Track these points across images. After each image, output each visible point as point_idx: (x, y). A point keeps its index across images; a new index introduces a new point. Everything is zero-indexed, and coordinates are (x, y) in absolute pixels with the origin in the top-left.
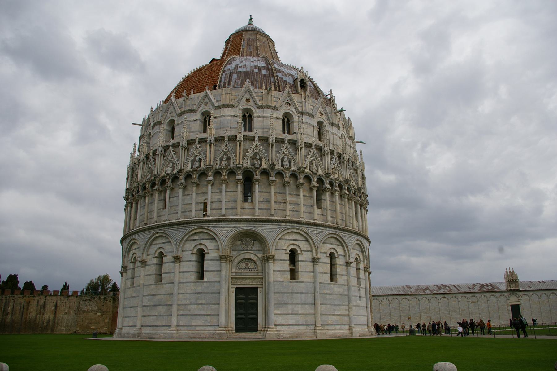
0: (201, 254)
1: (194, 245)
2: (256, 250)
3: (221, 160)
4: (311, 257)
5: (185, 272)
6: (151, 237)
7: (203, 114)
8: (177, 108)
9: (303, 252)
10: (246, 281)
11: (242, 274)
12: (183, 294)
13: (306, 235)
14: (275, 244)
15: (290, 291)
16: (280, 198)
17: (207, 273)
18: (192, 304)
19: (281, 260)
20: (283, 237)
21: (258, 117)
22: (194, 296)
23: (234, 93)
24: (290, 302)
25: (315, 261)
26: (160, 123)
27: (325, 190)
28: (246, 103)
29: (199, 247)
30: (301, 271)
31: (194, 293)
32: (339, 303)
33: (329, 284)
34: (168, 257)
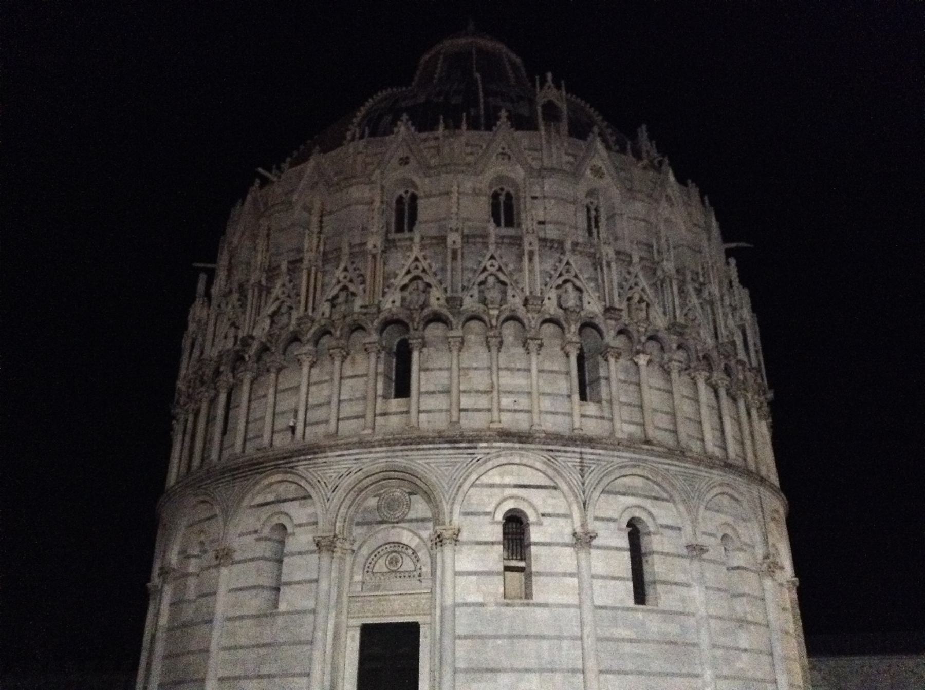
1: (264, 517)
2: (417, 520)
4: (568, 530)
9: (546, 521)
14: (460, 498)
15: (505, 632)
16: (480, 380)
19: (479, 543)
20: (485, 479)
21: (428, 196)
24: (506, 664)
25: (583, 540)
27: (604, 352)
30: (539, 574)
32: (667, 668)
33: (628, 609)
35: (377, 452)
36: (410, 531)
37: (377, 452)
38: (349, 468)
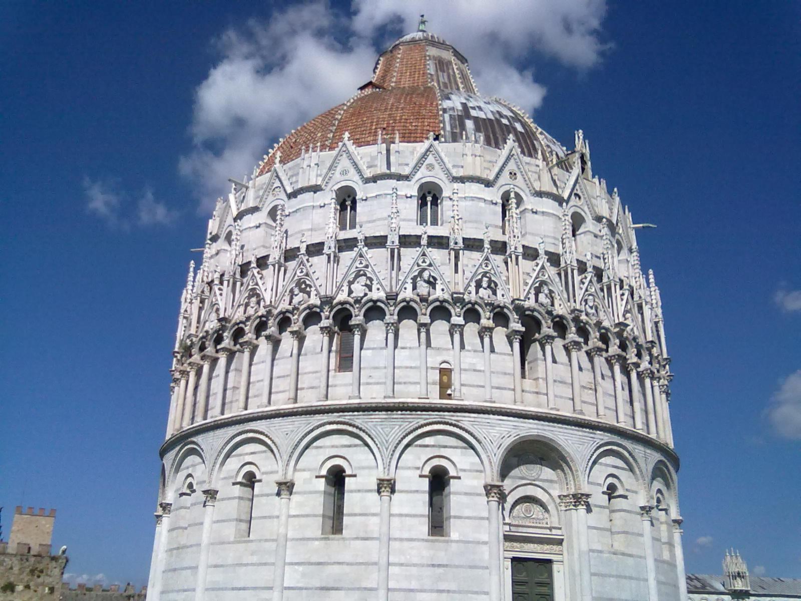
0: (439, 481)
2: (547, 481)
3: (479, 285)
5: (406, 515)
6: (312, 431)
7: (421, 187)
8: (363, 166)
10: (531, 547)
11: (520, 529)
12: (402, 565)
13: (631, 459)
15: (614, 573)
17: (458, 521)
18: (421, 591)
22: (429, 571)
23: (488, 158)
26: (316, 189)
28: (510, 181)
29: (436, 462)
31: (428, 566)
34: (358, 479)
35: (530, 423)
36: (542, 488)
37: (530, 423)
38: (509, 432)
